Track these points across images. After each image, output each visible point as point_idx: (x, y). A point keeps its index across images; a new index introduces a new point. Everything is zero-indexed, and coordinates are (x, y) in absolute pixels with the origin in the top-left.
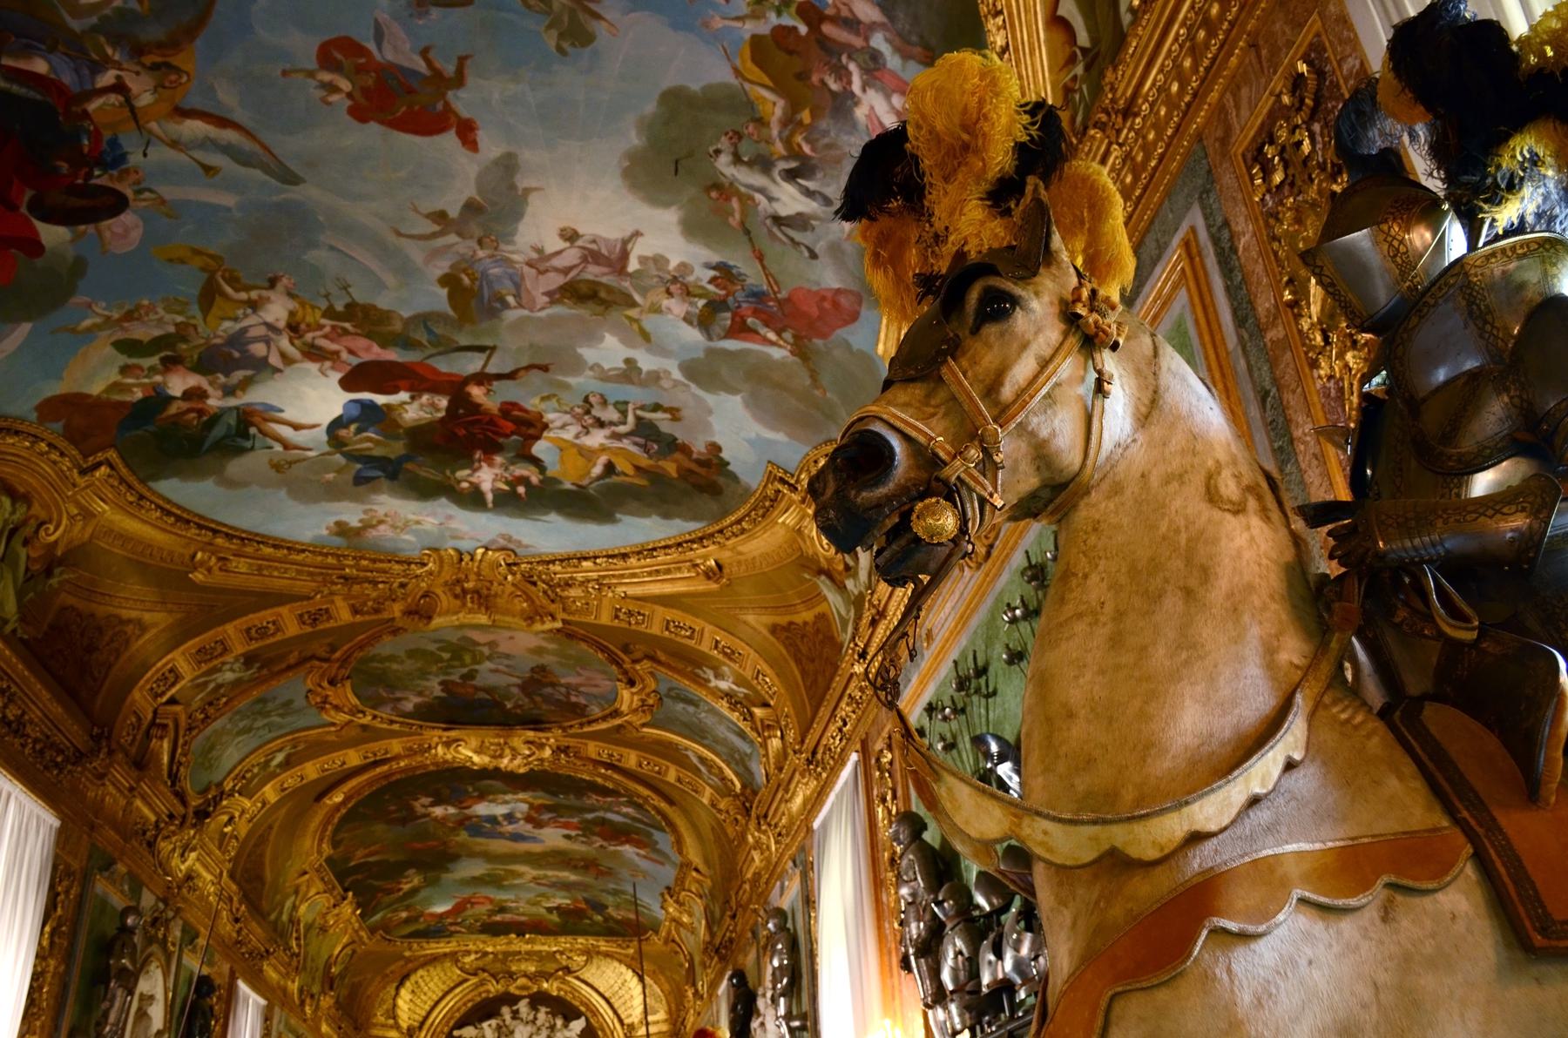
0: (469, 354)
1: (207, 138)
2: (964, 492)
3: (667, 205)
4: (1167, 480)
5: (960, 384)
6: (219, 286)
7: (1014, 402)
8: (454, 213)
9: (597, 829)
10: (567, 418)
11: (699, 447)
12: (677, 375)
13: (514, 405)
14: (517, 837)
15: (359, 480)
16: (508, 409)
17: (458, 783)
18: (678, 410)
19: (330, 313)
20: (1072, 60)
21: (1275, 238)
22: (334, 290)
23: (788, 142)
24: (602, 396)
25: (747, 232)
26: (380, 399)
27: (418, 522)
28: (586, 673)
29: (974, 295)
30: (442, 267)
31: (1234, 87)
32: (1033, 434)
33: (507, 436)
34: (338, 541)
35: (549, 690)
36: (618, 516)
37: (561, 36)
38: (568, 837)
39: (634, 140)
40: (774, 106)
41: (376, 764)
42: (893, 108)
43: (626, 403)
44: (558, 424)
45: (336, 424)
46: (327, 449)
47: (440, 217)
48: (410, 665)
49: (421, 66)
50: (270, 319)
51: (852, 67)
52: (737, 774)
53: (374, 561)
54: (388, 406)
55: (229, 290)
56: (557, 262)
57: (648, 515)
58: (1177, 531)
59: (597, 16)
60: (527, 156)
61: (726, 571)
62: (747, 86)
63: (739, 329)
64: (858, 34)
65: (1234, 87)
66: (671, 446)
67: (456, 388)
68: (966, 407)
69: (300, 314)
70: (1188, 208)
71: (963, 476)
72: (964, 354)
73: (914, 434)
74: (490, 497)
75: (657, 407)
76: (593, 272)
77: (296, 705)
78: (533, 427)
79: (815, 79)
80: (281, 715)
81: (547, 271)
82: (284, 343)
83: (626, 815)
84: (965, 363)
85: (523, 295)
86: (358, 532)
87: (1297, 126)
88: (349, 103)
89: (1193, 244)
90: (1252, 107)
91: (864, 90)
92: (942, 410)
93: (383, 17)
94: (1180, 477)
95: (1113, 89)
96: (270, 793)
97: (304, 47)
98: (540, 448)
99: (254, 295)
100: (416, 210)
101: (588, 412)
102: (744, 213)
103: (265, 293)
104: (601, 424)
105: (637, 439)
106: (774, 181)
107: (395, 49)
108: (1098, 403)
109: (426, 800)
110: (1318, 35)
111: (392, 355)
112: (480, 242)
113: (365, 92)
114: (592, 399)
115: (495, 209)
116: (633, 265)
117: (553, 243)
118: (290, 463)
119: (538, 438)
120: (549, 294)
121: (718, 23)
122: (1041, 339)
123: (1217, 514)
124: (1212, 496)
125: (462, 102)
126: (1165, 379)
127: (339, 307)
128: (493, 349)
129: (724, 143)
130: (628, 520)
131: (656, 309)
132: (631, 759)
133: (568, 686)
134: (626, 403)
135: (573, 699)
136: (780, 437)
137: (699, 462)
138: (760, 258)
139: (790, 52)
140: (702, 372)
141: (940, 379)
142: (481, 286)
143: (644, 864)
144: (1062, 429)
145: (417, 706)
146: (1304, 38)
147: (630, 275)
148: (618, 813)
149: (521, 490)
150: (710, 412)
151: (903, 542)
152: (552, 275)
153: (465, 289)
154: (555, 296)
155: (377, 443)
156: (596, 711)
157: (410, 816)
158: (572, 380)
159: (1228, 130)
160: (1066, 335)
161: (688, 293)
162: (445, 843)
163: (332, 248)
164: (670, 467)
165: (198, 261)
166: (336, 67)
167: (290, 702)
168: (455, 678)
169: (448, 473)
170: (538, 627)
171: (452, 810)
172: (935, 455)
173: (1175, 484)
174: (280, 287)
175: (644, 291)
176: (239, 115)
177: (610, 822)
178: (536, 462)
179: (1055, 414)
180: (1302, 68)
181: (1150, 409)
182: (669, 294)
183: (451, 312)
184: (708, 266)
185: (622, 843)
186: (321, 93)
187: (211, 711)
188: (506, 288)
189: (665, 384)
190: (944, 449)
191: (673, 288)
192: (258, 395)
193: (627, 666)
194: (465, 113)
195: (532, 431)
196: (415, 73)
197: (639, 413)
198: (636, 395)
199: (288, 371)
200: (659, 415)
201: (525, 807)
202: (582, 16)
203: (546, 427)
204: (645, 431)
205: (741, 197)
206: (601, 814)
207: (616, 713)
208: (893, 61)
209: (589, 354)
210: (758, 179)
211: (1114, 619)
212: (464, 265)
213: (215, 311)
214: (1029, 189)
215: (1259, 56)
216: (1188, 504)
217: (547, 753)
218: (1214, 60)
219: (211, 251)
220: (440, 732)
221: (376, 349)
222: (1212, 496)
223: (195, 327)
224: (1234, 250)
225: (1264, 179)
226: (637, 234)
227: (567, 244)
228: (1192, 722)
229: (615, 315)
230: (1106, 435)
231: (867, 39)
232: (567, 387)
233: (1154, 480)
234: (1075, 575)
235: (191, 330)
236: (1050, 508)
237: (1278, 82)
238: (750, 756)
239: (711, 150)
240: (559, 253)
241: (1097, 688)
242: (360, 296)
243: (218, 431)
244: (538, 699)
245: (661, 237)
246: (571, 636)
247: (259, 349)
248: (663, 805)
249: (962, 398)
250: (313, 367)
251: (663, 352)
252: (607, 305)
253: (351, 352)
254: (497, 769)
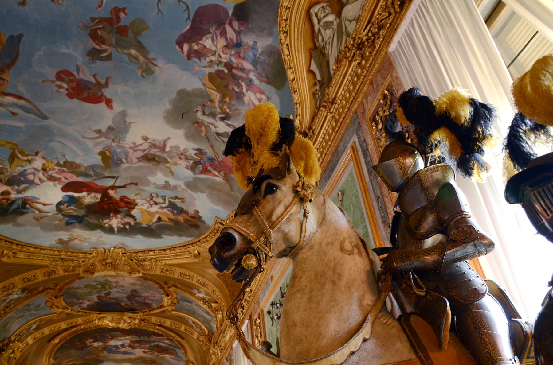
0: (109, 179)
1: (14, 103)
2: (260, 252)
3: (180, 128)
4: (328, 245)
5: (259, 215)
6: (16, 154)
7: (277, 221)
8: (104, 130)
9: (155, 349)
10: (144, 201)
11: (191, 212)
12: (183, 187)
13: (125, 197)
14: (125, 353)
15: (68, 224)
16: (123, 198)
17: (103, 333)
18: (184, 199)
19: (58, 164)
20: (315, 84)
21: (379, 146)
22: (60, 156)
23: (221, 108)
24: (157, 194)
25: (208, 138)
26: (76, 195)
27: (89, 239)
29: (264, 186)
30: (100, 149)
31: (366, 96)
32: (283, 231)
33: (123, 208)
34: (59, 245)
35: (137, 298)
36: (163, 236)
37: (143, 71)
38: (145, 352)
39: (168, 106)
40: (216, 96)
41: (72, 327)
42: (257, 97)
43: (165, 196)
44: (141, 203)
45: (59, 204)
46: (56, 212)
47: (99, 131)
48: (86, 290)
49: (93, 80)
50: (35, 166)
51: (243, 84)
52: (206, 327)
53: (73, 253)
54: (79, 197)
55: (20, 156)
56: (141, 148)
57: (173, 235)
58: (331, 262)
59: (155, 65)
60: (130, 111)
61: (201, 255)
62: (207, 89)
63: (205, 171)
64: (245, 73)
65: (366, 96)
66: (181, 211)
67: (104, 191)
68: (261, 223)
69: (47, 164)
70: (353, 135)
71: (259, 246)
72: (260, 205)
73: (243, 233)
74: (116, 229)
75: (176, 198)
76: (153, 151)
77: (41, 306)
78: (131, 205)
79: (230, 87)
80: (35, 310)
81: (137, 151)
82: (41, 175)
83: (166, 343)
84: (261, 208)
85: (129, 159)
86: (67, 242)
87: (385, 111)
88: (66, 92)
89: (354, 147)
90: (372, 104)
91: (247, 92)
92: (253, 224)
93: (80, 64)
94: (332, 243)
95: (328, 95)
96: (30, 340)
97: (51, 73)
98: (134, 212)
99: (30, 158)
100: (90, 129)
101: (152, 199)
102: (206, 132)
103: (34, 157)
104: (156, 203)
105: (169, 209)
106: (216, 121)
107: (84, 74)
108: (305, 220)
109: (91, 340)
110: (391, 82)
111: (81, 179)
112: (113, 141)
113: (73, 88)
114: (153, 195)
115: (118, 130)
116: (168, 149)
117: (139, 141)
118: (42, 218)
119: (133, 208)
120: (138, 158)
121: (197, 68)
122: (286, 200)
123: (344, 255)
124: (342, 249)
125: (107, 93)
126: (328, 211)
127: (62, 162)
128: (118, 177)
129: (199, 108)
131: (176, 164)
132: (168, 323)
133: (144, 297)
134: (165, 196)
135: (146, 301)
136: (220, 208)
137: (191, 217)
138: (212, 147)
139: (222, 79)
140: (192, 186)
141: (252, 214)
142: (113, 156)
143: (173, 361)
144: (292, 229)
145: (88, 306)
146: (386, 83)
147: (167, 152)
148: (163, 343)
149: (127, 227)
150: (195, 199)
151: (239, 269)
152: (139, 152)
153: (108, 156)
154: (140, 159)
155: (74, 210)
156: (155, 305)
157: (86, 346)
158: (146, 188)
159: (364, 110)
160: (294, 197)
161: (187, 158)
162: (98, 356)
163: (59, 142)
164: (181, 219)
165: (9, 146)
166: (62, 80)
167: (39, 305)
168: (103, 295)
169: (101, 221)
170: (133, 276)
171: (101, 344)
172: (250, 239)
173: (330, 246)
174: (39, 155)
175: (172, 158)
176: (26, 95)
177: (161, 346)
178: (133, 217)
179: (290, 225)
180: (386, 92)
181: (323, 221)
183: (102, 165)
184: (194, 149)
185: (165, 354)
186: (57, 88)
187: (7, 310)
188: (122, 157)
189: (179, 189)
190: (253, 238)
191: (182, 157)
192: (30, 193)
193: (166, 289)
194: (108, 96)
195: (131, 206)
196: (90, 82)
197: (170, 200)
199: (42, 185)
200: (177, 200)
201: (128, 342)
202: (150, 65)
203: (136, 204)
204: (172, 206)
205: (205, 126)
206: (157, 343)
207: (162, 306)
208: (256, 82)
209: (152, 179)
210: (211, 120)
211: (309, 292)
212: (107, 148)
213: (14, 163)
214: (283, 148)
215: (373, 87)
216: (334, 252)
217: (137, 321)
218: (359, 87)
219: (14, 142)
220: (97, 315)
221: (75, 177)
222: (342, 249)
223: (7, 169)
224: (367, 149)
225: (376, 127)
226: (169, 138)
227: (144, 141)
228: (334, 326)
229: (161, 166)
230: (307, 230)
231: (248, 75)
232: (144, 190)
233: (324, 245)
234: (297, 277)
235: (5, 170)
236: (290, 254)
237: (379, 96)
238: (211, 321)
239: (195, 110)
240: (141, 144)
241: (303, 316)
242: (69, 159)
243: (14, 206)
244: (133, 302)
245: (178, 139)
246: (145, 279)
247: (31, 177)
248: (180, 339)
249: (259, 220)
250: (51, 183)
251: (178, 178)
252: (158, 162)
253: (65, 178)
254: (118, 328)
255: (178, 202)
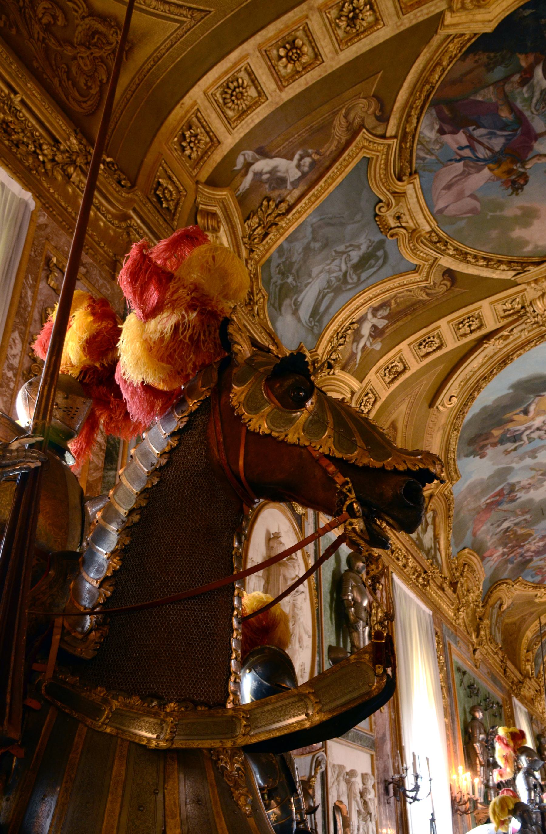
11: (490, 451)
24: (542, 439)
25: (512, 512)
28: (468, 203)
36: (511, 391)
40: (520, 532)
43: (530, 442)
57: (494, 402)
63: (500, 493)
66: (502, 441)
75: (515, 449)
104: (538, 429)
130: (505, 392)
134: (530, 442)
135: (461, 138)
137: (485, 445)
138: (505, 511)
161: (523, 488)
164: (497, 433)
175: (539, 479)
182: (530, 484)
184: (520, 497)
197: (522, 442)
198: (528, 448)
200: (513, 447)
204: (516, 438)
210: (515, 521)
251: (523, 468)
255: (510, 446)
